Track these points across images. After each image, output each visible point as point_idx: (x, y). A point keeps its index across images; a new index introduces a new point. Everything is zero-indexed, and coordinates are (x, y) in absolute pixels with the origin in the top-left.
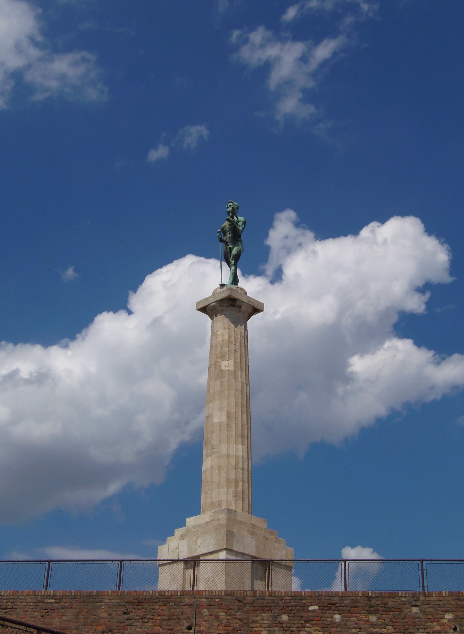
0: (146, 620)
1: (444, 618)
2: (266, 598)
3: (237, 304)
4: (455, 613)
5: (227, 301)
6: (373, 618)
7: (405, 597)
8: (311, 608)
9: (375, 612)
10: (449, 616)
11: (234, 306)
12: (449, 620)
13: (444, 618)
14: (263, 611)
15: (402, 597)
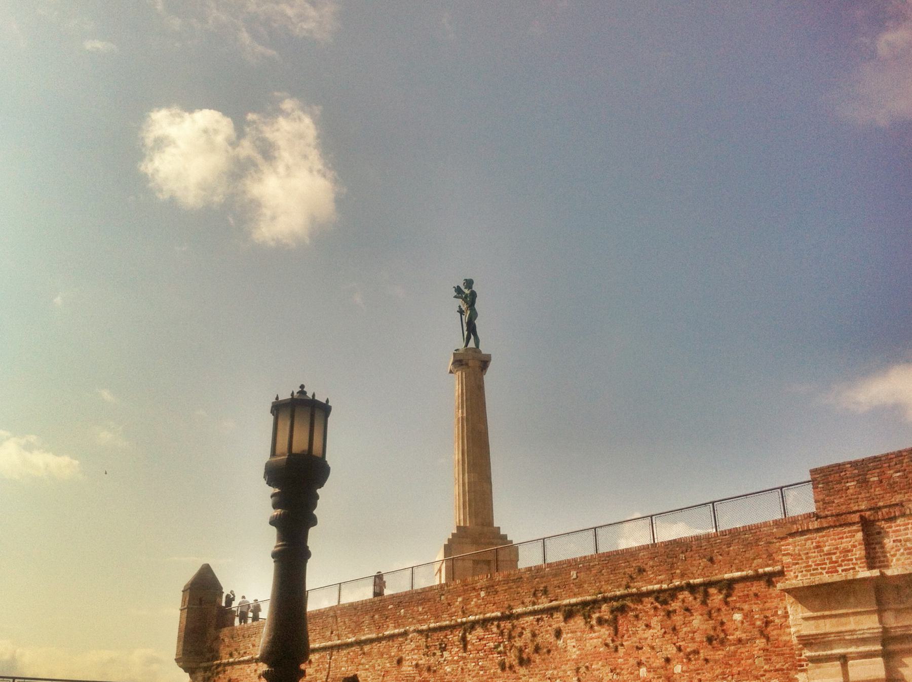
0: (312, 631)
1: (457, 601)
2: (368, 604)
3: (464, 363)
4: (463, 597)
5: (457, 363)
6: (420, 609)
7: (437, 589)
8: (390, 607)
9: (421, 604)
10: (460, 599)
11: (462, 365)
12: (460, 602)
13: (457, 601)
14: (366, 614)
15: (435, 589)
